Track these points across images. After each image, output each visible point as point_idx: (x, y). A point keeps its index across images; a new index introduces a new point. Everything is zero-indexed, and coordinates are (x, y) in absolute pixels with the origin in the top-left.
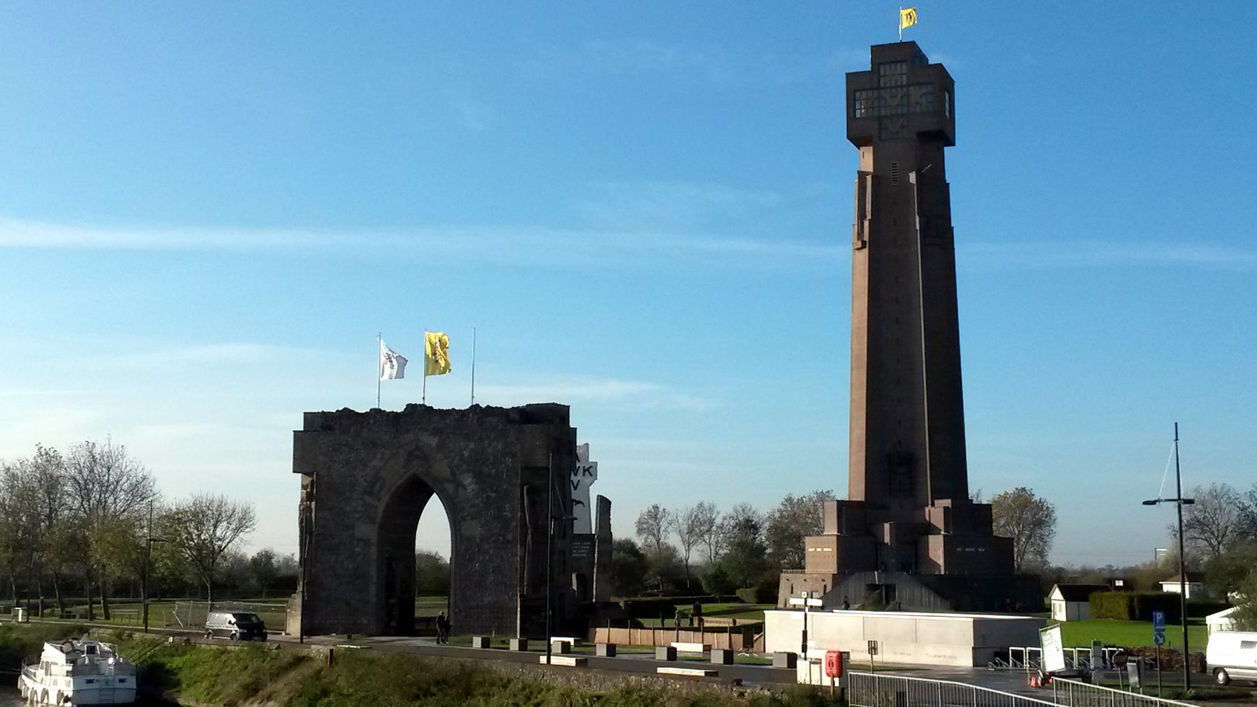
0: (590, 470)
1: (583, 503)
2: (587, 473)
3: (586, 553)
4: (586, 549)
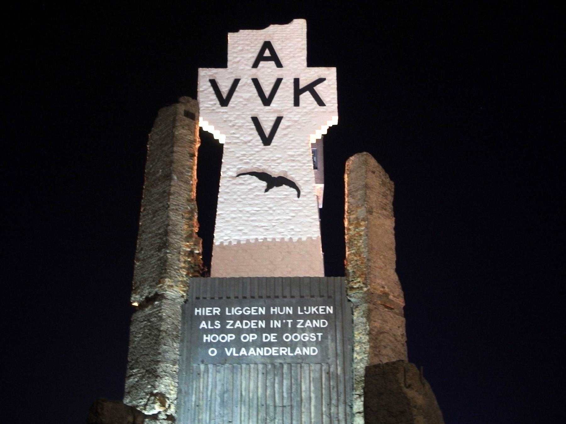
0: (318, 88)
1: (292, 184)
2: (306, 97)
3: (317, 343)
4: (316, 330)
